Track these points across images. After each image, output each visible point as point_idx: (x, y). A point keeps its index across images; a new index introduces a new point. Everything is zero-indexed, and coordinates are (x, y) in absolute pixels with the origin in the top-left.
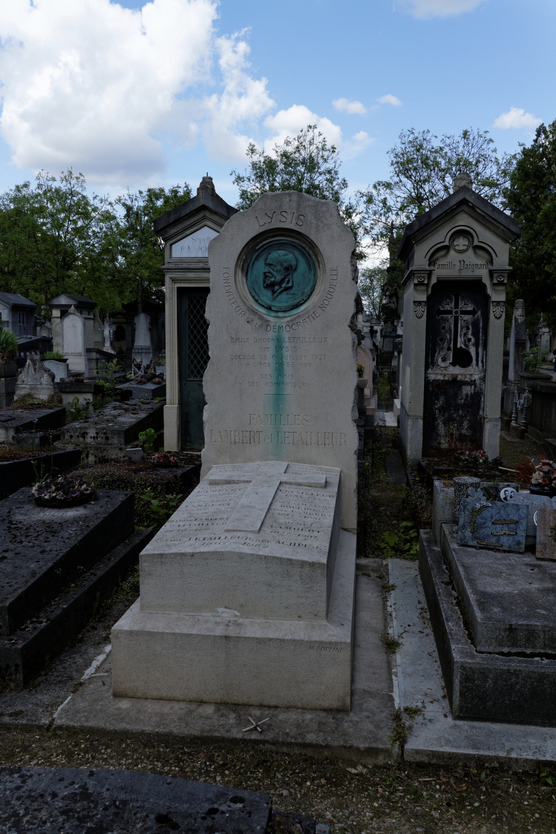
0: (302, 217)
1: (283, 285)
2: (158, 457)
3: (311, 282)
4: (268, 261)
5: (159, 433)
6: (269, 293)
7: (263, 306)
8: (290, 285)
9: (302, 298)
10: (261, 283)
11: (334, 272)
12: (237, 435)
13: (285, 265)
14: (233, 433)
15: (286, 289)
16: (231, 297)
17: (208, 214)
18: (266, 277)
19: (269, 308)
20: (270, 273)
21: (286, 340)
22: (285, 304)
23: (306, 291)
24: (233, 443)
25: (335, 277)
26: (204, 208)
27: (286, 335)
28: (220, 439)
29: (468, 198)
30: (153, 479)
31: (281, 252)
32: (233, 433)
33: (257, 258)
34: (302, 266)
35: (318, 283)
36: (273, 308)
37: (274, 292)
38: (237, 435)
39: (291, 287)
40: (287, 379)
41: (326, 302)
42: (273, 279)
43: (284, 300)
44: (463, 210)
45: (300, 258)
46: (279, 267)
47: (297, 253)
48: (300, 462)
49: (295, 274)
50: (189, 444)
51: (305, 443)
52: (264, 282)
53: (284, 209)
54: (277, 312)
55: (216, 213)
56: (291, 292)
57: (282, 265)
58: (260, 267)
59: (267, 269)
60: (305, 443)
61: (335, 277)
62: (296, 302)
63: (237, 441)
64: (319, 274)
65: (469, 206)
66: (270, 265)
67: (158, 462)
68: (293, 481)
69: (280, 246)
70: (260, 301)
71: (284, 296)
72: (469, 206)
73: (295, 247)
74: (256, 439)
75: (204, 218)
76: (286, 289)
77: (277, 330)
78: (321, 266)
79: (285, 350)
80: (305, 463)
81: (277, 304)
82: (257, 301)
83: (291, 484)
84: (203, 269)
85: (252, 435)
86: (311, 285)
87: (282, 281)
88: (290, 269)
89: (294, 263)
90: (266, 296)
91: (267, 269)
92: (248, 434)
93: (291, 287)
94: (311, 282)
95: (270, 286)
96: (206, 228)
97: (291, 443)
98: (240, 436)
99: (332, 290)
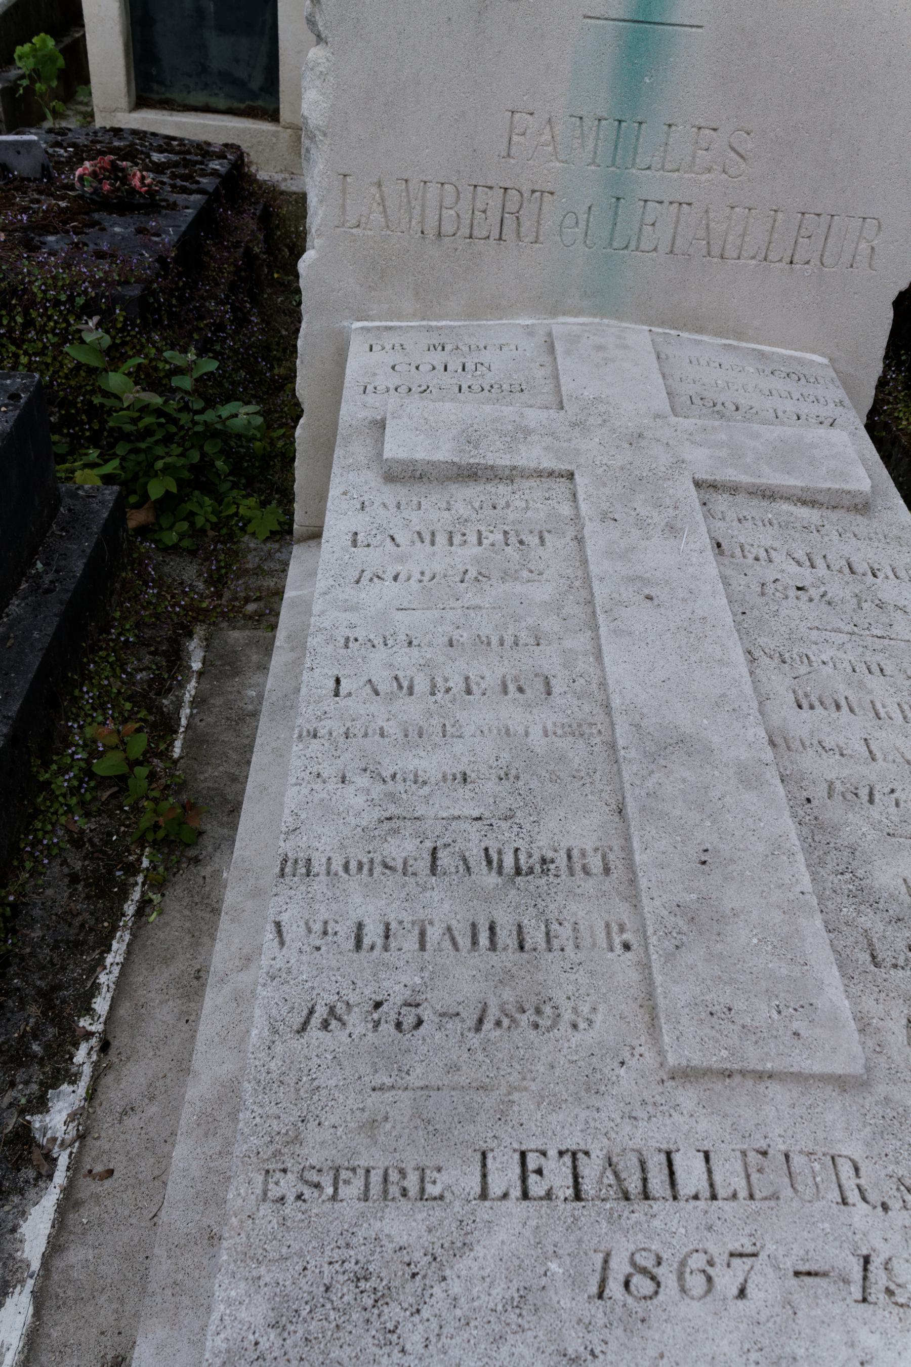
2: (94, 174)
5: (67, 40)
12: (449, 200)
14: (433, 188)
24: (431, 233)
28: (377, 217)
30: (96, 284)
32: (433, 188)
38: (449, 200)
48: (683, 327)
50: (156, 87)
51: (716, 250)
60: (716, 250)
63: (448, 228)
67: (96, 191)
68: (745, 479)
74: (527, 224)
80: (701, 330)
83: (734, 489)
85: (511, 207)
92: (494, 200)
97: (664, 247)
98: (464, 206)
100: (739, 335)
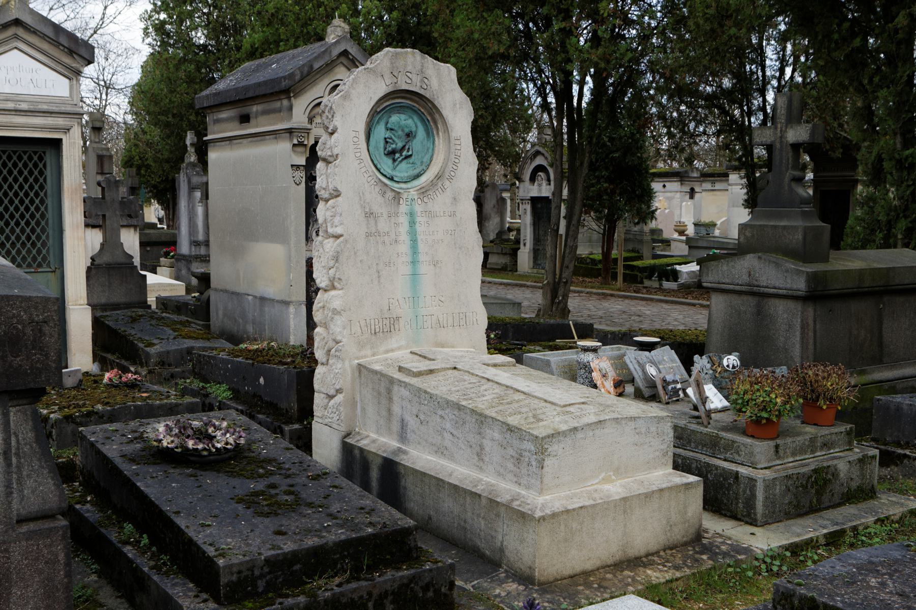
0: (426, 81)
1: (404, 153)
3: (430, 151)
4: (389, 126)
6: (390, 161)
7: (385, 176)
8: (410, 153)
9: (421, 168)
10: (382, 150)
11: (458, 142)
13: (407, 130)
14: (372, 322)
15: (407, 157)
16: (363, 165)
17: (20, 32)
18: (387, 142)
19: (391, 179)
20: (391, 138)
21: (419, 214)
22: (406, 175)
23: (425, 160)
25: (459, 147)
26: (17, 22)
27: (418, 208)
29: (350, 50)
31: (403, 117)
33: (378, 122)
34: (421, 133)
35: (436, 152)
36: (395, 179)
37: (394, 160)
39: (411, 156)
40: (422, 257)
41: (453, 174)
42: (394, 146)
43: (404, 170)
44: (341, 63)
45: (419, 124)
46: (400, 133)
47: (416, 118)
49: (415, 141)
52: (385, 149)
53: (409, 69)
54: (398, 182)
55: (34, 32)
56: (411, 160)
57: (403, 130)
58: (380, 132)
59: (388, 134)
61: (459, 147)
62: (416, 172)
63: (377, 330)
64: (437, 142)
65: (349, 58)
66: (392, 129)
69: (400, 109)
70: (382, 171)
71: (404, 165)
72: (349, 58)
73: (415, 111)
74: (396, 326)
75: (16, 37)
76: (407, 157)
77: (409, 203)
78: (441, 134)
79: (417, 225)
81: (399, 175)
82: (379, 170)
84: (16, 111)
86: (430, 154)
87: (404, 147)
88: (410, 135)
89: (414, 129)
90: (386, 164)
91: (388, 134)
92: (388, 322)
93: (411, 156)
94: (430, 151)
95: (391, 154)
96: (15, 51)
99: (457, 161)
100: (453, 347)
